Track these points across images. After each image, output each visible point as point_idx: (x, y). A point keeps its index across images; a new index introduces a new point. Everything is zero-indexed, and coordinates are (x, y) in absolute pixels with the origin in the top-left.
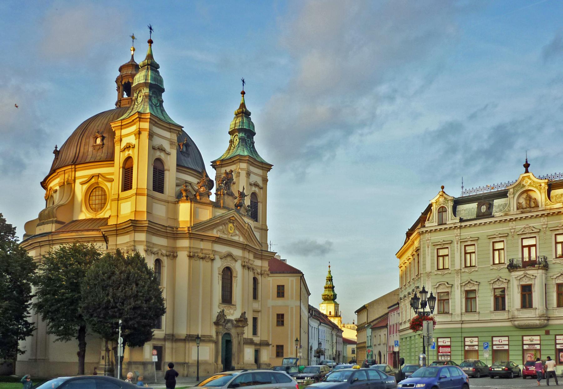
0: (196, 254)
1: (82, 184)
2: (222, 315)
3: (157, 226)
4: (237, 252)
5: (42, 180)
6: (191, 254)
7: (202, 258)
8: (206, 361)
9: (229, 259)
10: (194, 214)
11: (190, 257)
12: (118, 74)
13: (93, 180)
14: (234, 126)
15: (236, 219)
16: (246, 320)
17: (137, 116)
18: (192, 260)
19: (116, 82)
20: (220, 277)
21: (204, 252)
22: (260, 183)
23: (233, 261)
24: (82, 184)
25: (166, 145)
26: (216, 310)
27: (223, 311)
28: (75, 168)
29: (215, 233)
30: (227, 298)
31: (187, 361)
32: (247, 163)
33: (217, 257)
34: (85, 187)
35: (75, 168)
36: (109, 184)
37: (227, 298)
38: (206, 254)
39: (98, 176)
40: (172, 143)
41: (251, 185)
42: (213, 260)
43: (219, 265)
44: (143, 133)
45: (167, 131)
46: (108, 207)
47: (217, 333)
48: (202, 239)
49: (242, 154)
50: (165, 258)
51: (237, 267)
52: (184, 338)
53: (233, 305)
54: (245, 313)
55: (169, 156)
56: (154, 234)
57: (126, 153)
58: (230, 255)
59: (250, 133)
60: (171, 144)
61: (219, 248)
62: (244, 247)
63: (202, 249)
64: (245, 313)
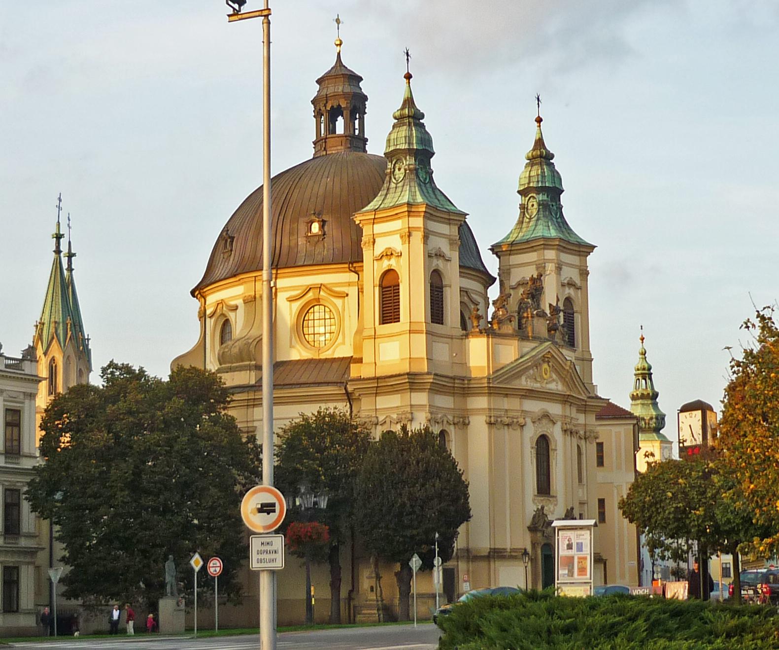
0: (499, 420)
3: (444, 379)
6: (493, 420)
7: (508, 425)
9: (544, 421)
10: (492, 355)
11: (490, 424)
13: (310, 295)
14: (527, 181)
15: (553, 356)
17: (406, 209)
18: (494, 430)
20: (534, 452)
21: (510, 414)
22: (577, 280)
23: (551, 425)
25: (445, 248)
26: (531, 508)
27: (543, 508)
28: (277, 274)
29: (524, 383)
30: (544, 488)
32: (558, 249)
33: (529, 420)
34: (297, 305)
35: (277, 274)
36: (338, 302)
38: (513, 418)
39: (320, 287)
40: (452, 243)
41: (563, 285)
43: (531, 433)
44: (414, 233)
45: (443, 223)
47: (534, 545)
48: (507, 393)
49: (547, 235)
50: (452, 427)
51: (556, 434)
52: (486, 554)
53: (553, 497)
54: (572, 509)
55: (449, 263)
56: (438, 392)
57: (385, 264)
58: (546, 416)
59: (555, 192)
60: (451, 244)
62: (565, 400)
63: (507, 411)
64: (572, 509)
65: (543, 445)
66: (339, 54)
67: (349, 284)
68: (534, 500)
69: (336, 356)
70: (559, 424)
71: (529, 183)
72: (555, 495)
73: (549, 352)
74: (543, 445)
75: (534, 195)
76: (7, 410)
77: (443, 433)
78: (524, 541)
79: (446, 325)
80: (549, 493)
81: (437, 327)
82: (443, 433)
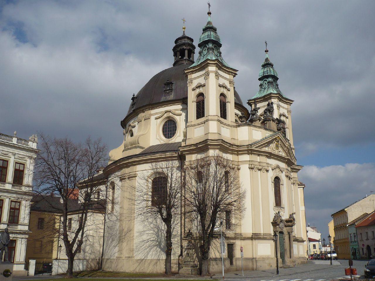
1: (156, 119)
2: (277, 216)
4: (283, 165)
9: (278, 170)
15: (280, 139)
19: (176, 42)
20: (273, 184)
24: (156, 119)
30: (278, 203)
31: (254, 257)
33: (270, 169)
37: (278, 203)
42: (267, 171)
43: (271, 175)
48: (259, 153)
51: (283, 176)
58: (278, 167)
65: (277, 180)
66: (184, 32)
69: (176, 141)
70: (284, 173)
71: (264, 74)
72: (284, 207)
73: (278, 136)
74: (277, 180)
75: (266, 79)
76: (16, 163)
78: (271, 230)
79: (228, 120)
80: (281, 206)
81: (222, 120)
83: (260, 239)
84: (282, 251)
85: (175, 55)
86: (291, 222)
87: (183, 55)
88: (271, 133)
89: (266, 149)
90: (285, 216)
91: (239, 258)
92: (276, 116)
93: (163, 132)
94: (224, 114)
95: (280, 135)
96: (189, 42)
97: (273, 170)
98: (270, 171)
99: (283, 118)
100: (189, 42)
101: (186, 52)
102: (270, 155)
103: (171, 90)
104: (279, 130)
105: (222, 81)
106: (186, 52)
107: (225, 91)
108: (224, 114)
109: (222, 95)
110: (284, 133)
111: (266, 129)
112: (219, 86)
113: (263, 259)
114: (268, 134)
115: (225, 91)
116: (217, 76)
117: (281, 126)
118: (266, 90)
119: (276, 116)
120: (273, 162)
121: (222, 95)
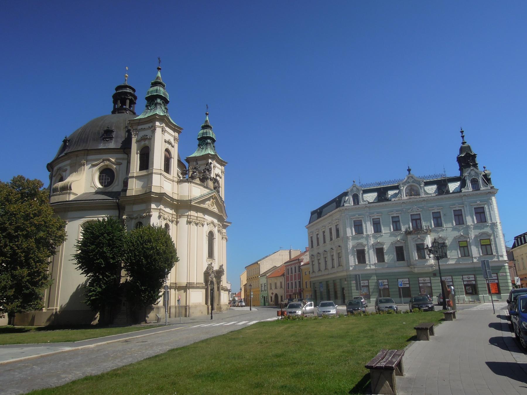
2: (210, 267)
4: (216, 221)
5: (49, 162)
8: (200, 303)
12: (115, 92)
16: (223, 270)
20: (207, 238)
27: (211, 264)
30: (211, 255)
37: (211, 255)
42: (203, 225)
43: (206, 229)
46: (116, 183)
54: (222, 265)
58: (213, 223)
61: (206, 217)
64: (222, 265)
67: (123, 159)
68: (207, 260)
70: (217, 227)
74: (211, 235)
77: (167, 226)
78: (201, 280)
82: (167, 226)
83: (193, 288)
84: (211, 298)
85: (115, 102)
86: (219, 273)
87: (124, 103)
88: (208, 191)
89: (202, 206)
90: (216, 267)
91: (173, 306)
92: (213, 175)
93: (100, 179)
94: (167, 168)
95: (215, 194)
96: (131, 91)
97: (208, 225)
98: (205, 226)
99: (218, 178)
100: (131, 91)
101: (128, 101)
102: (205, 211)
103: (111, 138)
104: (215, 188)
105: (167, 137)
106: (128, 101)
107: (170, 147)
108: (167, 168)
109: (167, 150)
110: (218, 192)
111: (204, 187)
112: (165, 142)
113: (196, 306)
114: (206, 191)
115: (170, 147)
116: (163, 131)
117: (216, 184)
118: (204, 150)
119: (213, 175)
120: (209, 218)
121: (167, 150)
